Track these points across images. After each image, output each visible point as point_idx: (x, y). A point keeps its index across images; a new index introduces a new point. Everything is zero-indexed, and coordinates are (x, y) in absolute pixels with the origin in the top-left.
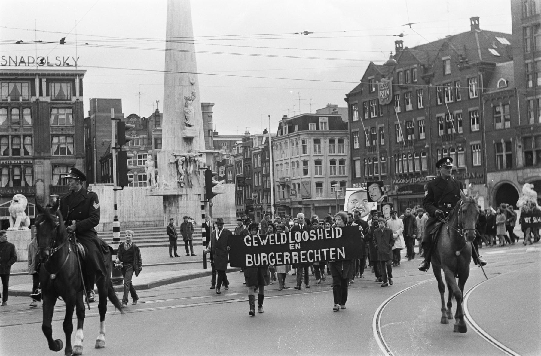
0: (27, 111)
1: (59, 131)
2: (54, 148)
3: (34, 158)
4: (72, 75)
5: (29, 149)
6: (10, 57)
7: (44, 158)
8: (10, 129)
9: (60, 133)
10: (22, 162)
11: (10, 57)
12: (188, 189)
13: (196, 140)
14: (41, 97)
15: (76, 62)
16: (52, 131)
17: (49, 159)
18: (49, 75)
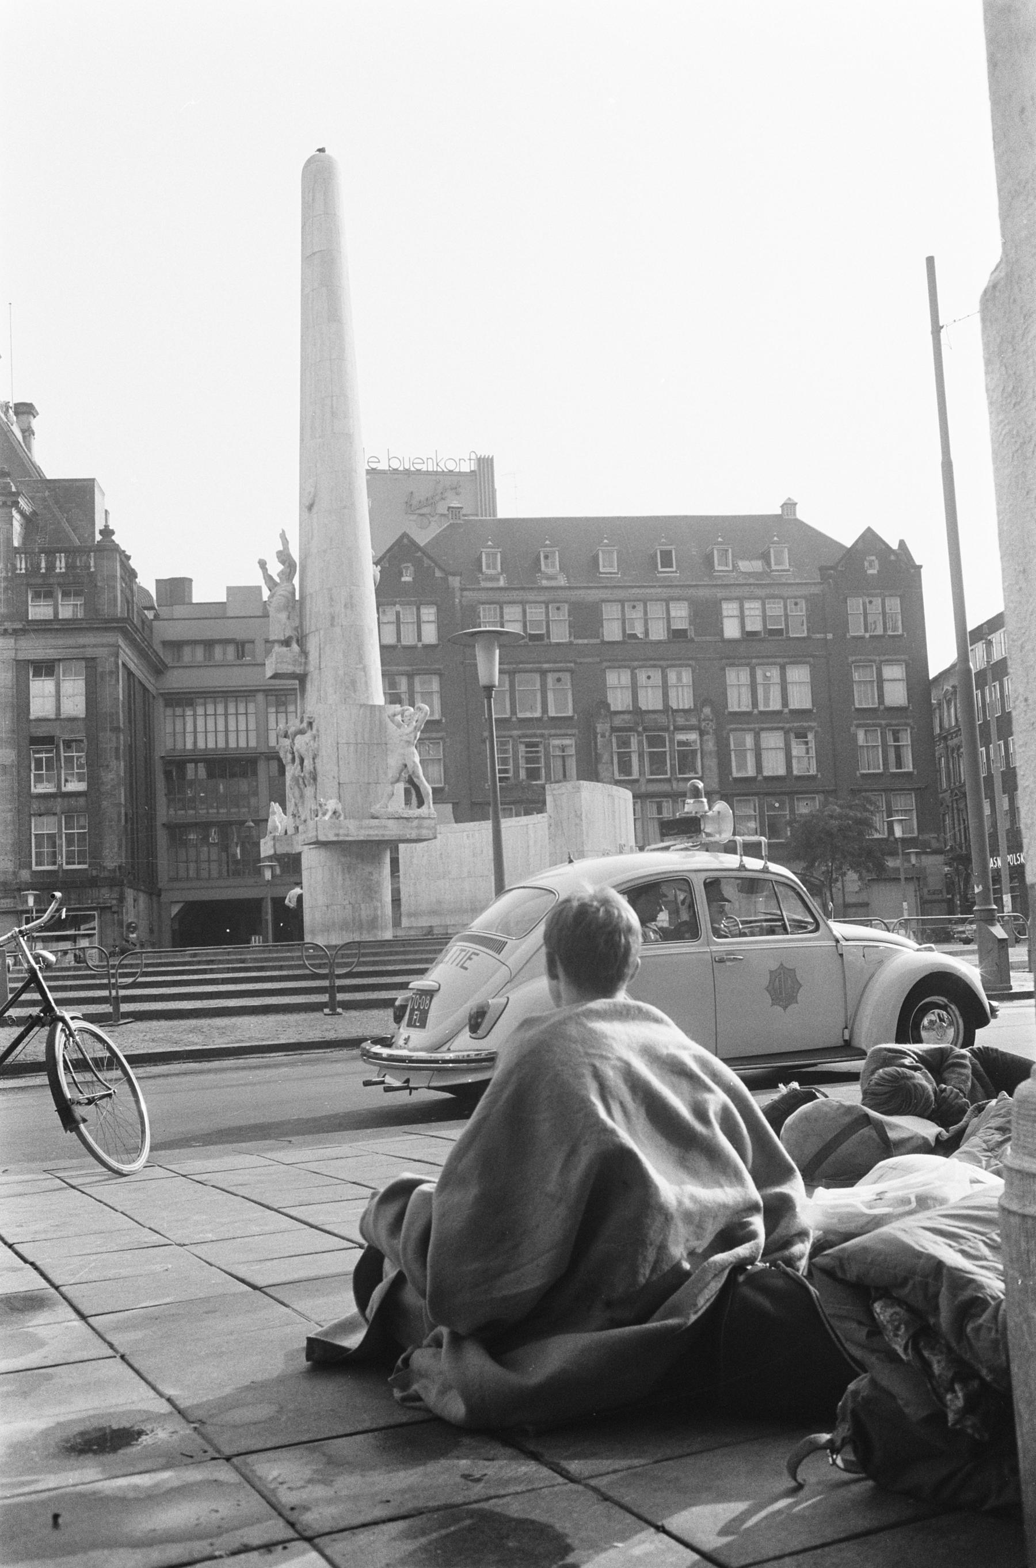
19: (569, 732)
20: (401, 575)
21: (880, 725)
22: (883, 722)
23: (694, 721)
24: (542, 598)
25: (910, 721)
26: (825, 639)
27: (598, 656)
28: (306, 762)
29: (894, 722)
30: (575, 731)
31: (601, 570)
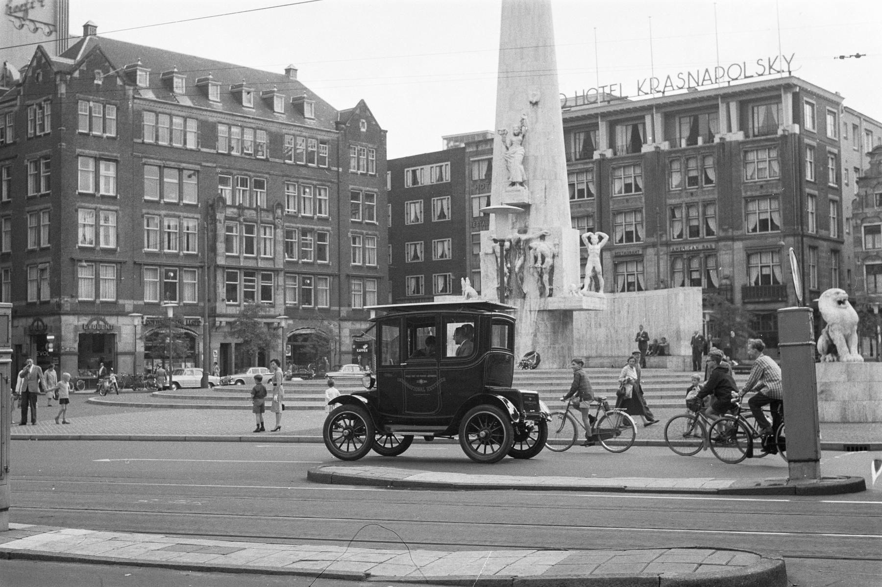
0: (710, 162)
1: (756, 190)
2: (753, 221)
3: (720, 239)
4: (772, 88)
5: (713, 225)
6: (689, 74)
7: (733, 239)
8: (684, 194)
9: (758, 194)
10: (700, 247)
11: (689, 74)
12: (519, 301)
13: (536, 209)
14: (730, 134)
15: (789, 64)
16: (746, 192)
17: (742, 240)
18: (742, 93)
19: (112, 208)
20: (94, 79)
21: (362, 234)
22: (365, 232)
23: (271, 218)
24: (183, 114)
25: (377, 233)
26: (338, 171)
27: (215, 162)
28: (547, 260)
29: (370, 233)
30: (198, 216)
31: (244, 104)
